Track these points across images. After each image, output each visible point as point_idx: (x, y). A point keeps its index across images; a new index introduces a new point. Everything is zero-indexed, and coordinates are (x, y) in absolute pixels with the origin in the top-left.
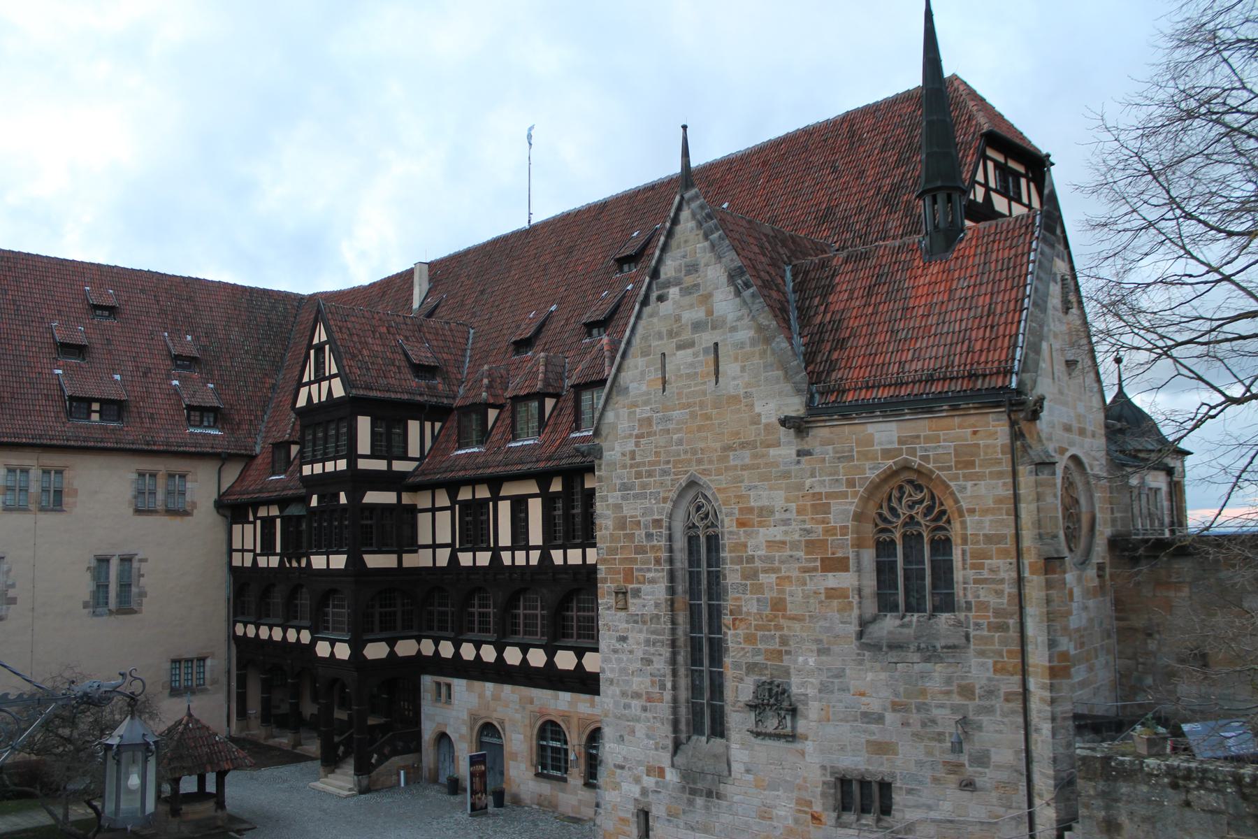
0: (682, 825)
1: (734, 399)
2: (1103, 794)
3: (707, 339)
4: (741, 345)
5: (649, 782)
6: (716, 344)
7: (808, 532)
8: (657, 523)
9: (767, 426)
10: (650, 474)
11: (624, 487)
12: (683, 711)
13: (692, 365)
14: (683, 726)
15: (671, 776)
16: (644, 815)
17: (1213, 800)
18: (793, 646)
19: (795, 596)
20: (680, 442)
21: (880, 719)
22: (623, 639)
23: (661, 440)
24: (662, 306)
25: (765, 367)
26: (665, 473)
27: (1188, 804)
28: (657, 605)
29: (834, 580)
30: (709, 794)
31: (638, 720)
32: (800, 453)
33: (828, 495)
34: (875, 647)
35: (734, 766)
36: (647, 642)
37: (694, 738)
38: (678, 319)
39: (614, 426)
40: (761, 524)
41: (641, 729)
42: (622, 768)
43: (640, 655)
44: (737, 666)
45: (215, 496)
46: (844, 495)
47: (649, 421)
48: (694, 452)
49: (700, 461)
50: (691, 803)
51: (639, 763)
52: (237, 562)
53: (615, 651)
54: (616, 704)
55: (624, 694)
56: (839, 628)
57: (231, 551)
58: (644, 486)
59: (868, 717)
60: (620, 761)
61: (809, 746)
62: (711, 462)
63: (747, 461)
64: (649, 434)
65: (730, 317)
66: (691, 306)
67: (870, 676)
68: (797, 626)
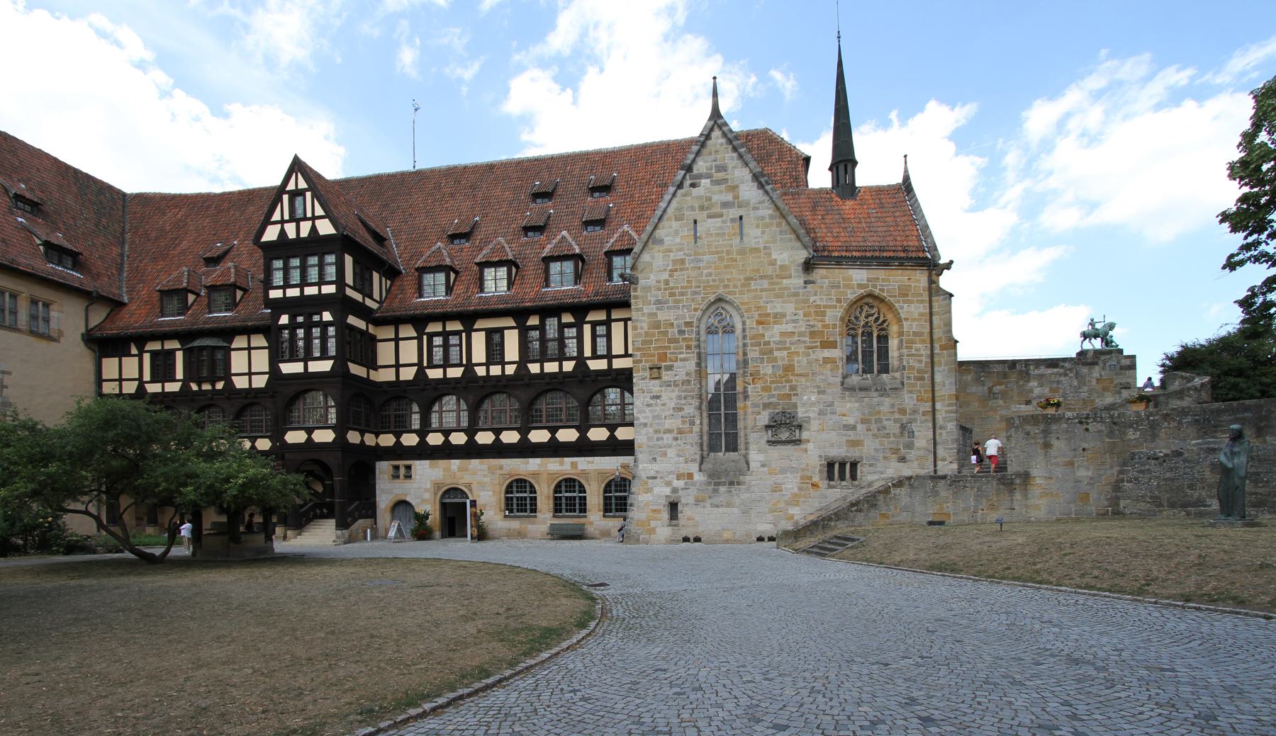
0: (708, 505)
1: (757, 250)
2: (1043, 431)
3: (734, 213)
4: (763, 218)
5: (680, 484)
6: (741, 218)
7: (812, 326)
8: (689, 324)
9: (781, 267)
10: (682, 294)
11: (658, 302)
12: (705, 438)
13: (721, 228)
14: (705, 448)
15: (698, 477)
16: (673, 507)
17: (1100, 427)
18: (799, 390)
19: (801, 363)
20: (710, 275)
21: (854, 428)
22: (658, 397)
23: (694, 273)
24: (694, 190)
25: (781, 232)
26: (696, 293)
27: (1087, 430)
28: (687, 374)
29: (827, 353)
30: (731, 483)
31: (670, 446)
32: (806, 282)
33: (825, 307)
34: (852, 389)
35: (752, 465)
36: (679, 397)
37: (712, 454)
38: (709, 199)
39: (650, 264)
40: (775, 323)
41: (671, 453)
42: (655, 478)
43: (673, 405)
44: (755, 405)
45: (83, 330)
46: (835, 307)
47: (682, 261)
48: (722, 281)
49: (726, 286)
50: (715, 491)
51: (670, 473)
52: (109, 388)
53: (648, 405)
54: (649, 439)
55: (656, 432)
56: (831, 380)
57: (100, 381)
58: (677, 302)
59: (848, 427)
60: (652, 474)
61: (810, 446)
62: (735, 286)
63: (766, 286)
64: (682, 270)
65: (753, 201)
66: (721, 192)
67: (849, 405)
68: (803, 379)
